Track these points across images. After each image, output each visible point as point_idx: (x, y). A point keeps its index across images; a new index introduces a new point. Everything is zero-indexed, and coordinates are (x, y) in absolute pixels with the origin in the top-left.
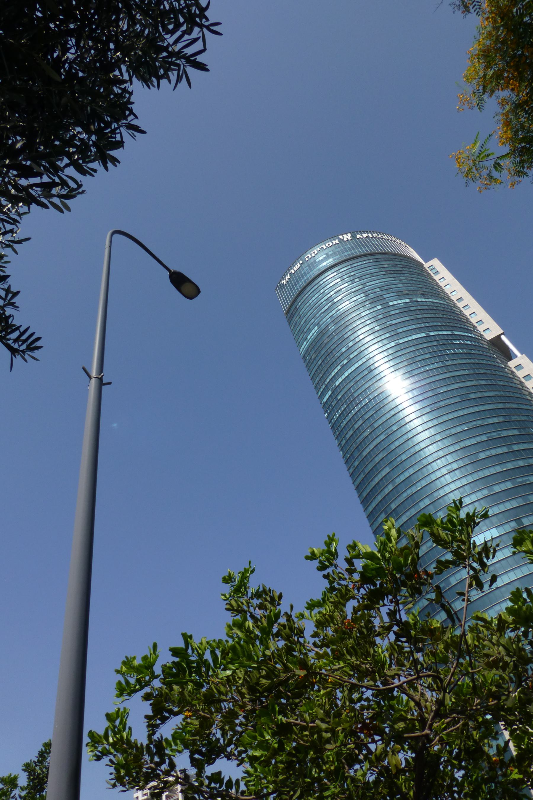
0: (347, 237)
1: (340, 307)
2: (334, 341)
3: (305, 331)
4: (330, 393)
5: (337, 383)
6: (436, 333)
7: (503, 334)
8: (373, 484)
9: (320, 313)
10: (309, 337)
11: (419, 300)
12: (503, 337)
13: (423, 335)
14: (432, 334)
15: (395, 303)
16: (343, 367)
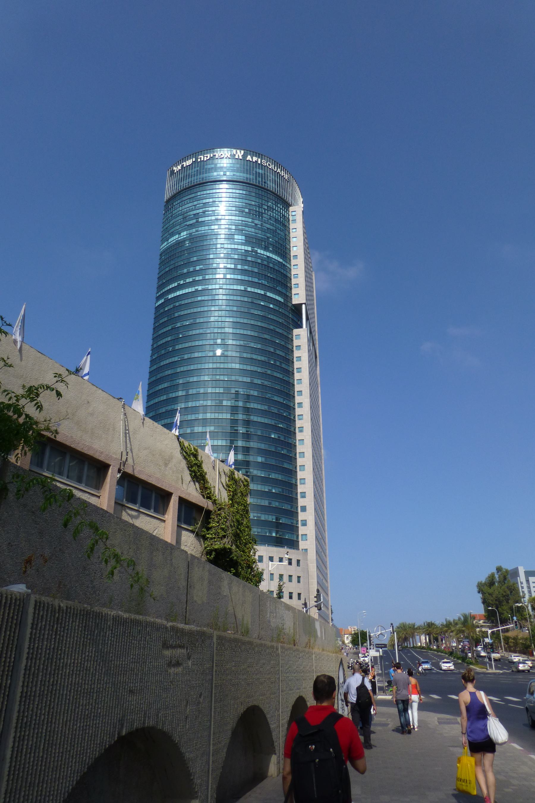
0: (240, 154)
1: (200, 229)
2: (183, 257)
3: (170, 232)
4: (163, 300)
5: (170, 297)
6: (252, 290)
7: (305, 304)
8: (157, 388)
9: (185, 224)
10: (170, 241)
11: (259, 251)
12: (304, 306)
13: (242, 288)
14: (249, 289)
15: (240, 247)
16: (179, 285)
